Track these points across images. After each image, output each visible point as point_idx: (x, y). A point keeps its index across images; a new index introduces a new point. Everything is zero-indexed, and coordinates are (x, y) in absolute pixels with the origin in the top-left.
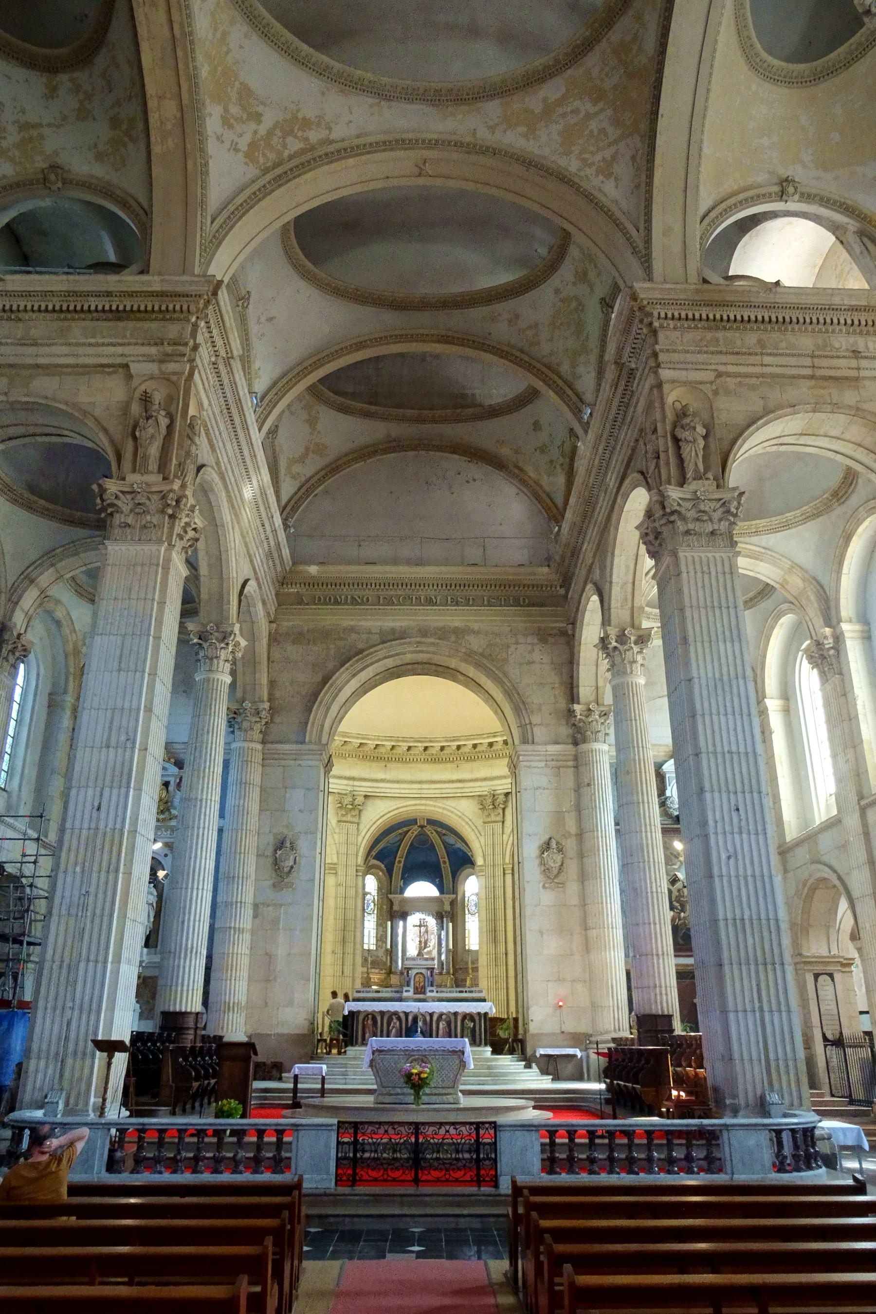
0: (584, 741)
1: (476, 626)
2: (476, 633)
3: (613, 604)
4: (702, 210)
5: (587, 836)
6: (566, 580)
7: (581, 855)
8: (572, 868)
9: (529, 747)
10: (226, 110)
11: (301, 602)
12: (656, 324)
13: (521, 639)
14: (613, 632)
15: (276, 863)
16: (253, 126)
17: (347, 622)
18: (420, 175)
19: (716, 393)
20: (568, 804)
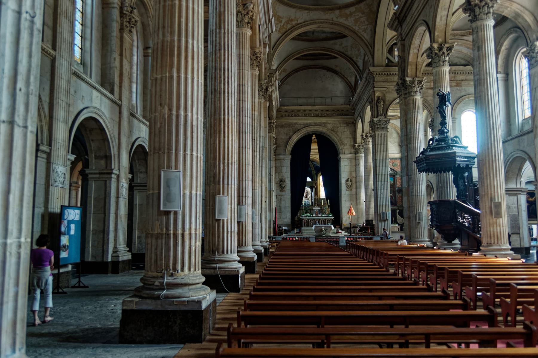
0: (358, 153)
1: (329, 122)
2: (329, 124)
3: (365, 127)
5: (358, 178)
6: (354, 109)
7: (356, 183)
8: (354, 185)
9: (344, 155)
11: (282, 116)
12: (374, 76)
13: (342, 125)
14: (364, 134)
15: (280, 185)
16: (280, 24)
17: (295, 122)
19: (386, 92)
20: (353, 170)
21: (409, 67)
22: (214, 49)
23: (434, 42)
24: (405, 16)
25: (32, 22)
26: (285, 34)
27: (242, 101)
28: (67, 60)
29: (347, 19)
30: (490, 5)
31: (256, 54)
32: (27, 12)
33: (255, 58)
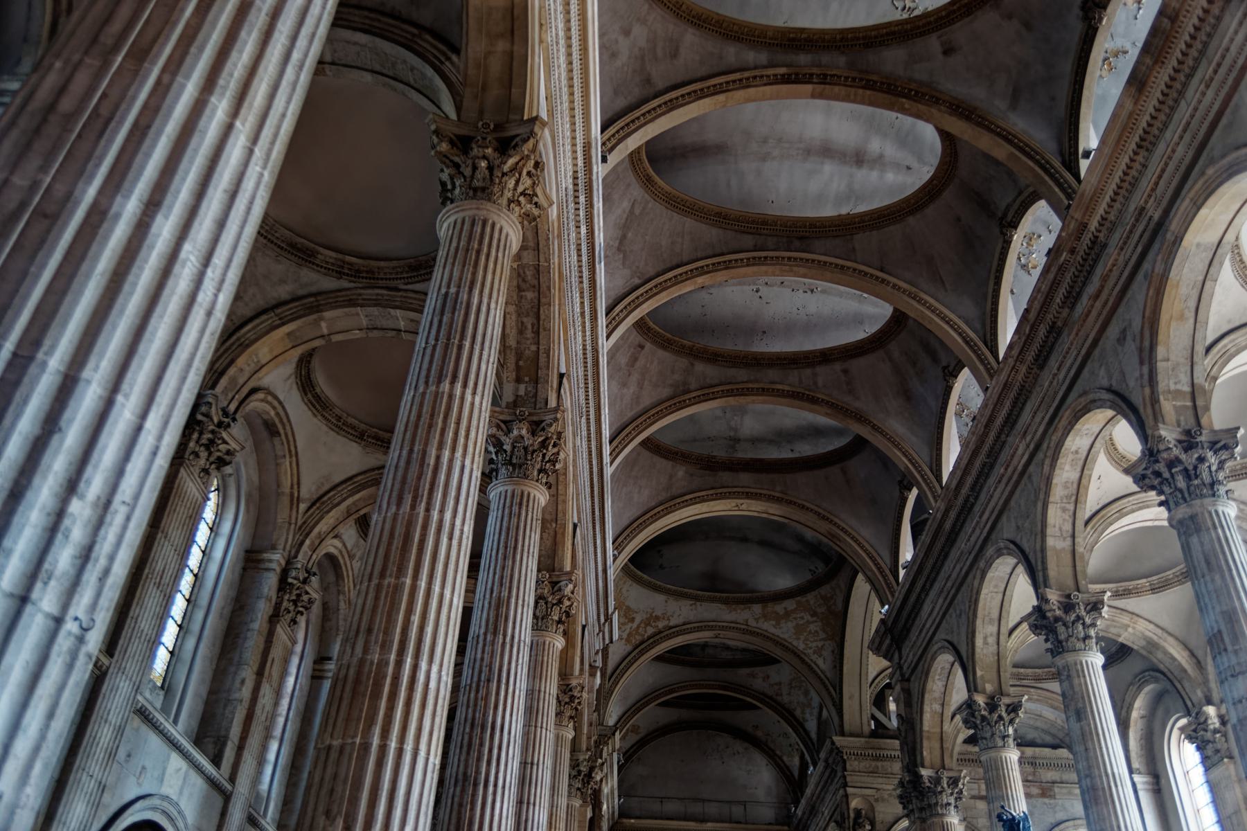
4: (870, 679)
16: (630, 625)
19: (877, 800)
21: (925, 743)
22: (475, 679)
23: (976, 690)
24: (907, 630)
25: (81, 640)
26: (639, 648)
27: (528, 803)
28: (131, 680)
29: (778, 623)
30: (1088, 621)
31: (571, 690)
32: (76, 619)
33: (567, 700)
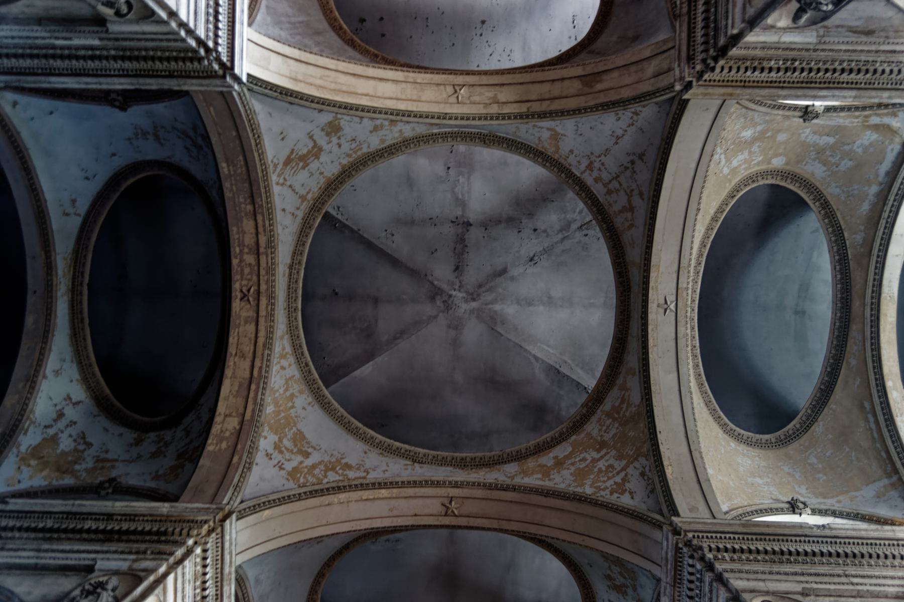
10: (280, 440)
16: (300, 458)
18: (446, 515)
